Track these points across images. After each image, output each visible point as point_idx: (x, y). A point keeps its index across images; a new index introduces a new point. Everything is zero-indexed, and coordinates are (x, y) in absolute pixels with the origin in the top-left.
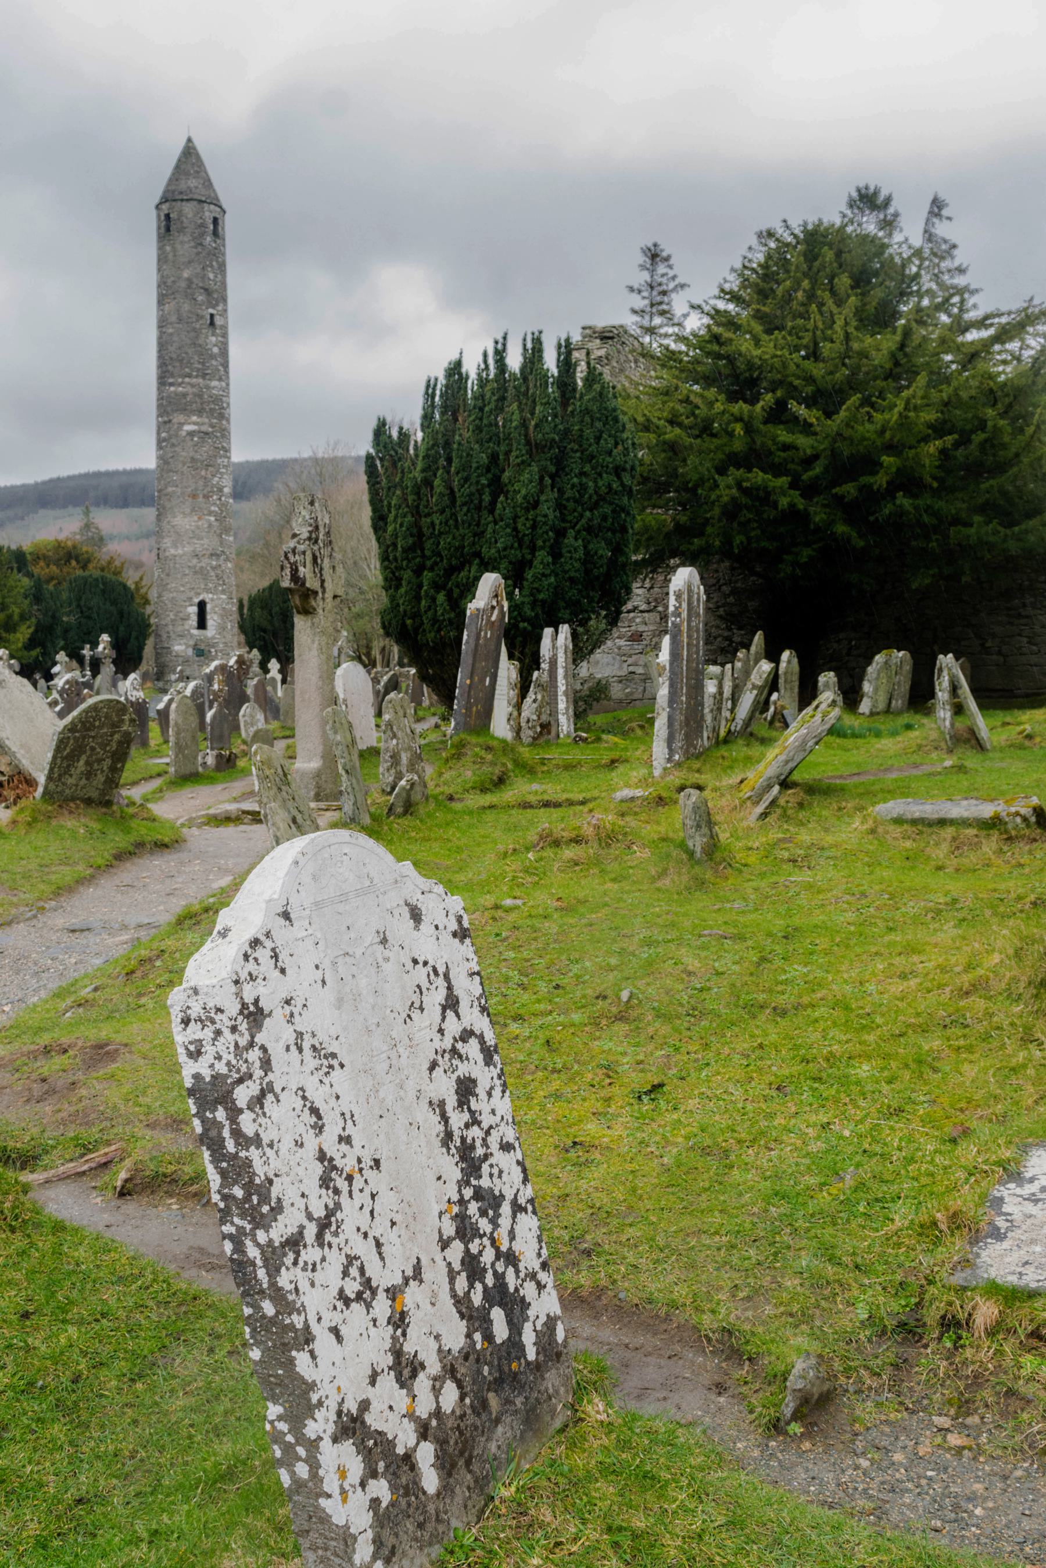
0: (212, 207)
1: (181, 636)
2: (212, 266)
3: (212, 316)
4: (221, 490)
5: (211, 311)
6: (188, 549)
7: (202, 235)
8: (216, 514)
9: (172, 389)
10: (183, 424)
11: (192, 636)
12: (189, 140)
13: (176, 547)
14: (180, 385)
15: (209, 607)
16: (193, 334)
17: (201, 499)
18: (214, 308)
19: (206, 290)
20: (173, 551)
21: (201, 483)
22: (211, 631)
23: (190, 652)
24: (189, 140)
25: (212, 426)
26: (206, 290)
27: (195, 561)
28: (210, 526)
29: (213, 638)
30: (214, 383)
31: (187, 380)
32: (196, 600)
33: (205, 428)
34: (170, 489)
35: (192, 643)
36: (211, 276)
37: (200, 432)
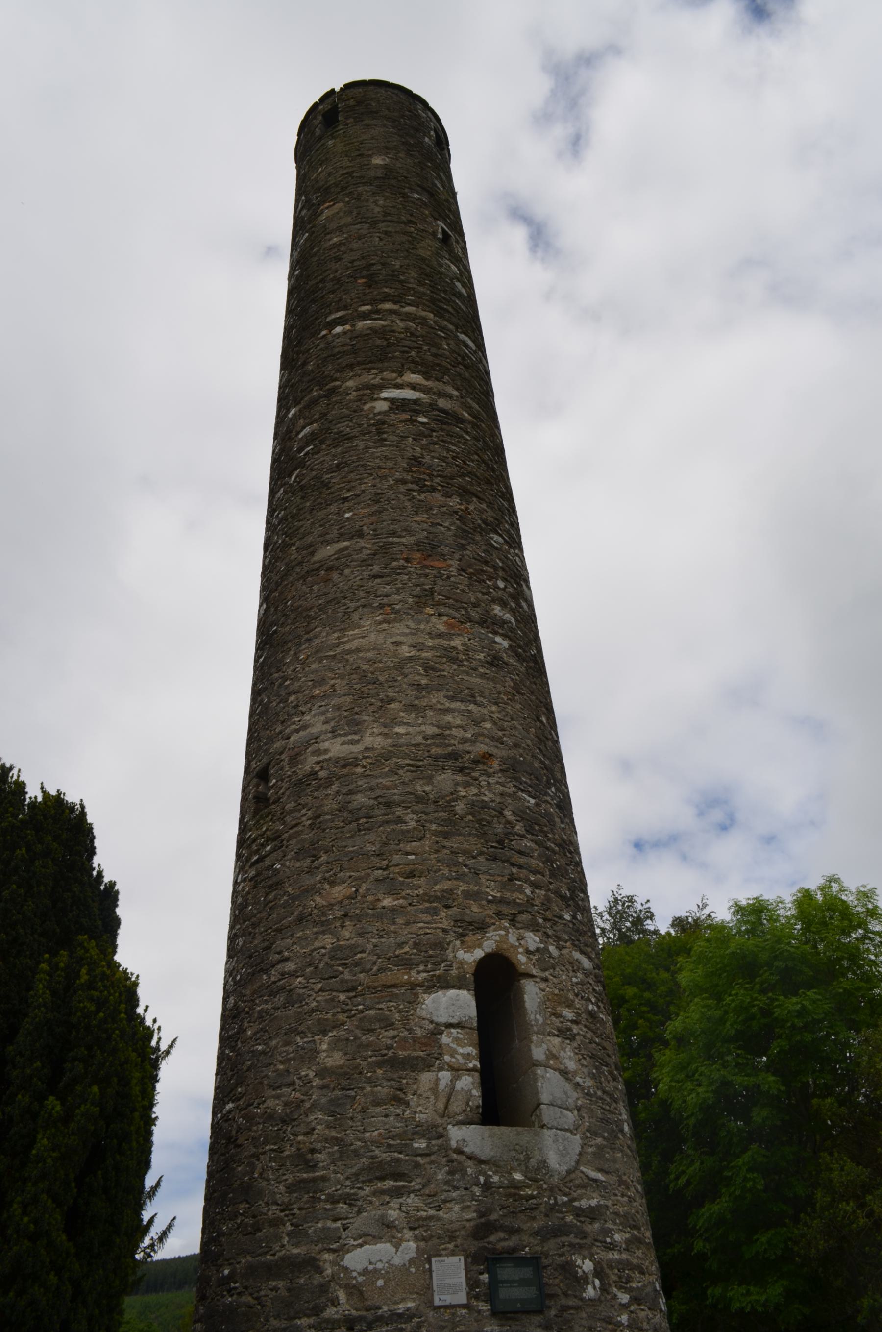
1: (392, 1174)
6: (411, 730)
9: (338, 329)
10: (381, 387)
11: (457, 1160)
13: (356, 726)
14: (365, 316)
15: (532, 994)
20: (336, 748)
22: (558, 1148)
23: (451, 1278)
27: (445, 780)
28: (495, 661)
29: (571, 1181)
31: (388, 306)
32: (471, 957)
33: (442, 403)
34: (328, 551)
35: (457, 1214)
37: (433, 406)
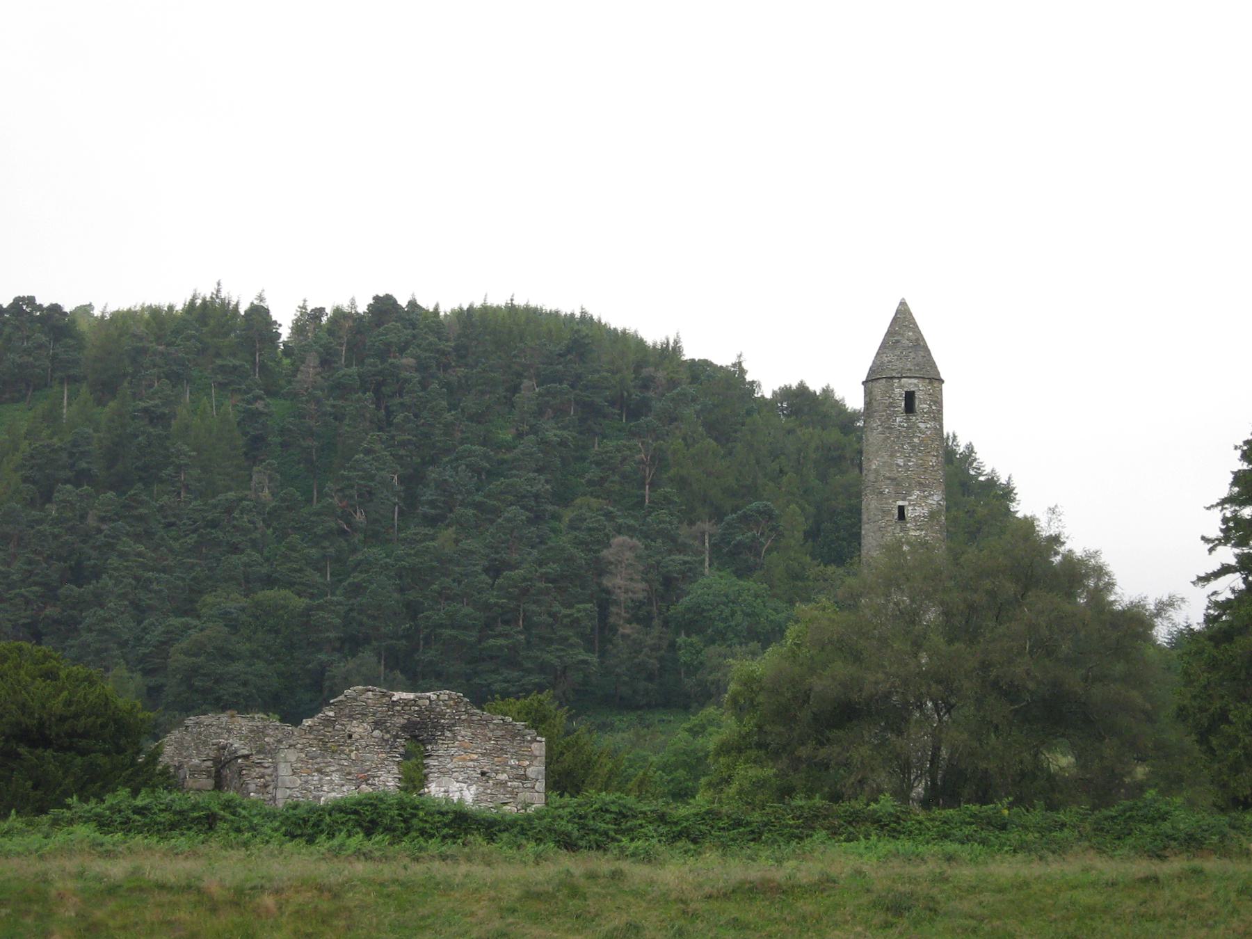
0: (903, 380)
3: (901, 509)
5: (901, 503)
7: (889, 417)
12: (903, 304)
16: (879, 534)
18: (904, 499)
24: (903, 304)
26: (893, 479)
36: (900, 462)
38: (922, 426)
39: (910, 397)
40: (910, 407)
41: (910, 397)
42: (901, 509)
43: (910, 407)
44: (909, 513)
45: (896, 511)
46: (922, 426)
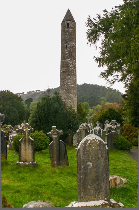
0: (67, 21)
2: (67, 34)
4: (67, 83)
5: (66, 44)
7: (65, 29)
8: (65, 89)
12: (69, 9)
17: (63, 86)
19: (65, 40)
21: (63, 83)
24: (69, 9)
25: (65, 70)
26: (65, 40)
30: (66, 60)
33: (63, 71)
36: (66, 37)
38: (70, 30)
39: (68, 24)
40: (68, 27)
41: (68, 24)
42: (66, 45)
43: (68, 27)
44: (68, 46)
45: (65, 46)
46: (70, 30)
